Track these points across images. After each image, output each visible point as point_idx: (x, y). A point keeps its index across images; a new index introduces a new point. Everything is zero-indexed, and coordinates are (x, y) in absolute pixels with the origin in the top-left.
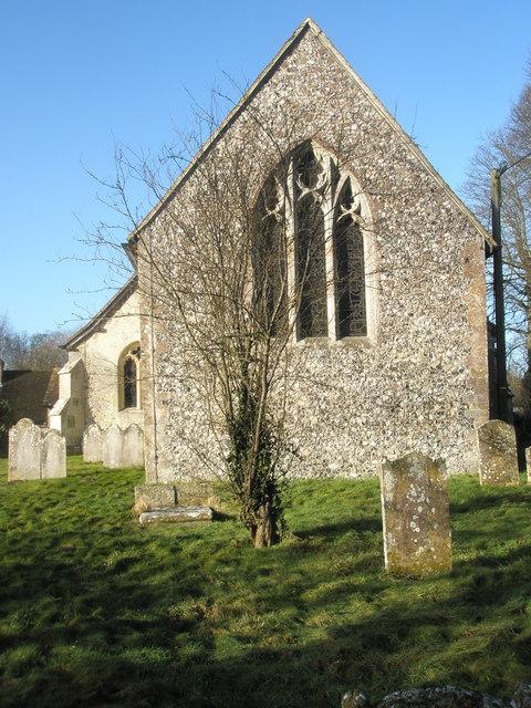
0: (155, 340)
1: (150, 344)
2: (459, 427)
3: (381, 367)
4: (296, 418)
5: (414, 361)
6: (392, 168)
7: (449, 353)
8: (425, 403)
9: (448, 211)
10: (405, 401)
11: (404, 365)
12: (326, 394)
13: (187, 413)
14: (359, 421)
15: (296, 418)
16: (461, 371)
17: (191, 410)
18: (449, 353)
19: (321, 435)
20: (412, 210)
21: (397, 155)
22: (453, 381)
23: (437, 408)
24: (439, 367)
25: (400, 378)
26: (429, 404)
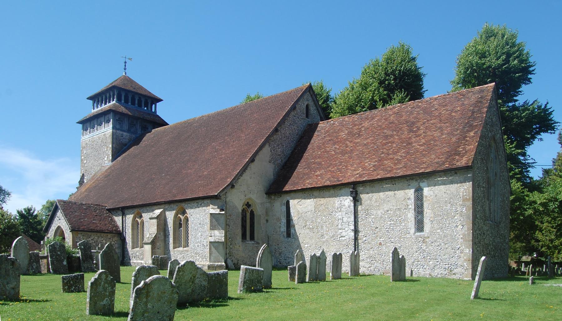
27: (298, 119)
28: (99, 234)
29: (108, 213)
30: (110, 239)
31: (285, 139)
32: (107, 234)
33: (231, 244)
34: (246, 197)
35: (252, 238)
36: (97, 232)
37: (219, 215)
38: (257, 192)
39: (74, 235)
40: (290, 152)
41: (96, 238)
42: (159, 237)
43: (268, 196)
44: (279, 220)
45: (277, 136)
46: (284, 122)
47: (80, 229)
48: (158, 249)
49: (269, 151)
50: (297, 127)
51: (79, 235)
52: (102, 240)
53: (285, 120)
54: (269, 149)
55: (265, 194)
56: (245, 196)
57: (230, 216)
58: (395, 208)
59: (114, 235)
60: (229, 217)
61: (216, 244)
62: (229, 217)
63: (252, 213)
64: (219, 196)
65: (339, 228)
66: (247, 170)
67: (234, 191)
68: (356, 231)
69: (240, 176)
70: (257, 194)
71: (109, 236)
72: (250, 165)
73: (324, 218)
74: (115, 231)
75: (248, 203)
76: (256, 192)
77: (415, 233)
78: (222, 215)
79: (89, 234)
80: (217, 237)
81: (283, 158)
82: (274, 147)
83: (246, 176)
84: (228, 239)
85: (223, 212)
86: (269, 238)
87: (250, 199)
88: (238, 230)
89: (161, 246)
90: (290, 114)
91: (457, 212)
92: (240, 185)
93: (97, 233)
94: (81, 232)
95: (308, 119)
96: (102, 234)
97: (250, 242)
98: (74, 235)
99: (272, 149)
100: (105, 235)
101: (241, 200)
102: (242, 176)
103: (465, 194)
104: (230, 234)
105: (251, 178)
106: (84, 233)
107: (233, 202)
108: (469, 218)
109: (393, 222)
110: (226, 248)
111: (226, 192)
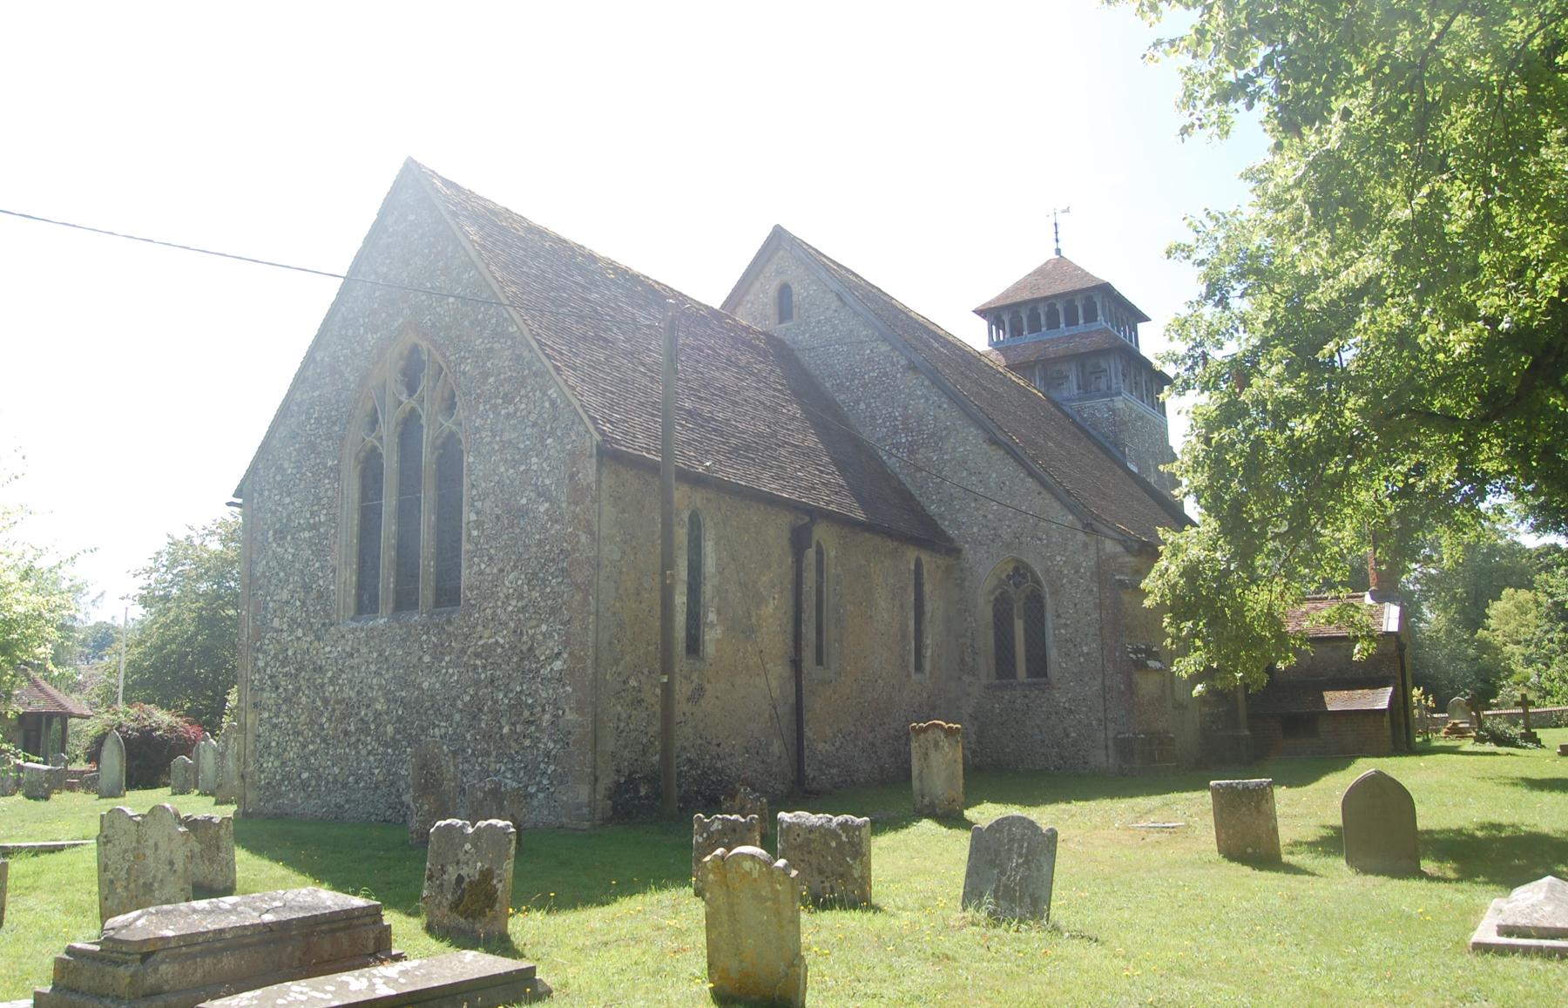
0: (251, 624)
2: (551, 745)
3: (463, 651)
4: (373, 727)
5: (501, 641)
6: (490, 350)
7: (544, 628)
8: (513, 707)
9: (553, 403)
10: (490, 703)
11: (489, 649)
12: (404, 694)
15: (373, 727)
16: (559, 654)
18: (544, 628)
19: (397, 752)
20: (511, 409)
21: (499, 330)
22: (545, 671)
23: (526, 713)
24: (531, 649)
25: (484, 667)
26: (517, 706)
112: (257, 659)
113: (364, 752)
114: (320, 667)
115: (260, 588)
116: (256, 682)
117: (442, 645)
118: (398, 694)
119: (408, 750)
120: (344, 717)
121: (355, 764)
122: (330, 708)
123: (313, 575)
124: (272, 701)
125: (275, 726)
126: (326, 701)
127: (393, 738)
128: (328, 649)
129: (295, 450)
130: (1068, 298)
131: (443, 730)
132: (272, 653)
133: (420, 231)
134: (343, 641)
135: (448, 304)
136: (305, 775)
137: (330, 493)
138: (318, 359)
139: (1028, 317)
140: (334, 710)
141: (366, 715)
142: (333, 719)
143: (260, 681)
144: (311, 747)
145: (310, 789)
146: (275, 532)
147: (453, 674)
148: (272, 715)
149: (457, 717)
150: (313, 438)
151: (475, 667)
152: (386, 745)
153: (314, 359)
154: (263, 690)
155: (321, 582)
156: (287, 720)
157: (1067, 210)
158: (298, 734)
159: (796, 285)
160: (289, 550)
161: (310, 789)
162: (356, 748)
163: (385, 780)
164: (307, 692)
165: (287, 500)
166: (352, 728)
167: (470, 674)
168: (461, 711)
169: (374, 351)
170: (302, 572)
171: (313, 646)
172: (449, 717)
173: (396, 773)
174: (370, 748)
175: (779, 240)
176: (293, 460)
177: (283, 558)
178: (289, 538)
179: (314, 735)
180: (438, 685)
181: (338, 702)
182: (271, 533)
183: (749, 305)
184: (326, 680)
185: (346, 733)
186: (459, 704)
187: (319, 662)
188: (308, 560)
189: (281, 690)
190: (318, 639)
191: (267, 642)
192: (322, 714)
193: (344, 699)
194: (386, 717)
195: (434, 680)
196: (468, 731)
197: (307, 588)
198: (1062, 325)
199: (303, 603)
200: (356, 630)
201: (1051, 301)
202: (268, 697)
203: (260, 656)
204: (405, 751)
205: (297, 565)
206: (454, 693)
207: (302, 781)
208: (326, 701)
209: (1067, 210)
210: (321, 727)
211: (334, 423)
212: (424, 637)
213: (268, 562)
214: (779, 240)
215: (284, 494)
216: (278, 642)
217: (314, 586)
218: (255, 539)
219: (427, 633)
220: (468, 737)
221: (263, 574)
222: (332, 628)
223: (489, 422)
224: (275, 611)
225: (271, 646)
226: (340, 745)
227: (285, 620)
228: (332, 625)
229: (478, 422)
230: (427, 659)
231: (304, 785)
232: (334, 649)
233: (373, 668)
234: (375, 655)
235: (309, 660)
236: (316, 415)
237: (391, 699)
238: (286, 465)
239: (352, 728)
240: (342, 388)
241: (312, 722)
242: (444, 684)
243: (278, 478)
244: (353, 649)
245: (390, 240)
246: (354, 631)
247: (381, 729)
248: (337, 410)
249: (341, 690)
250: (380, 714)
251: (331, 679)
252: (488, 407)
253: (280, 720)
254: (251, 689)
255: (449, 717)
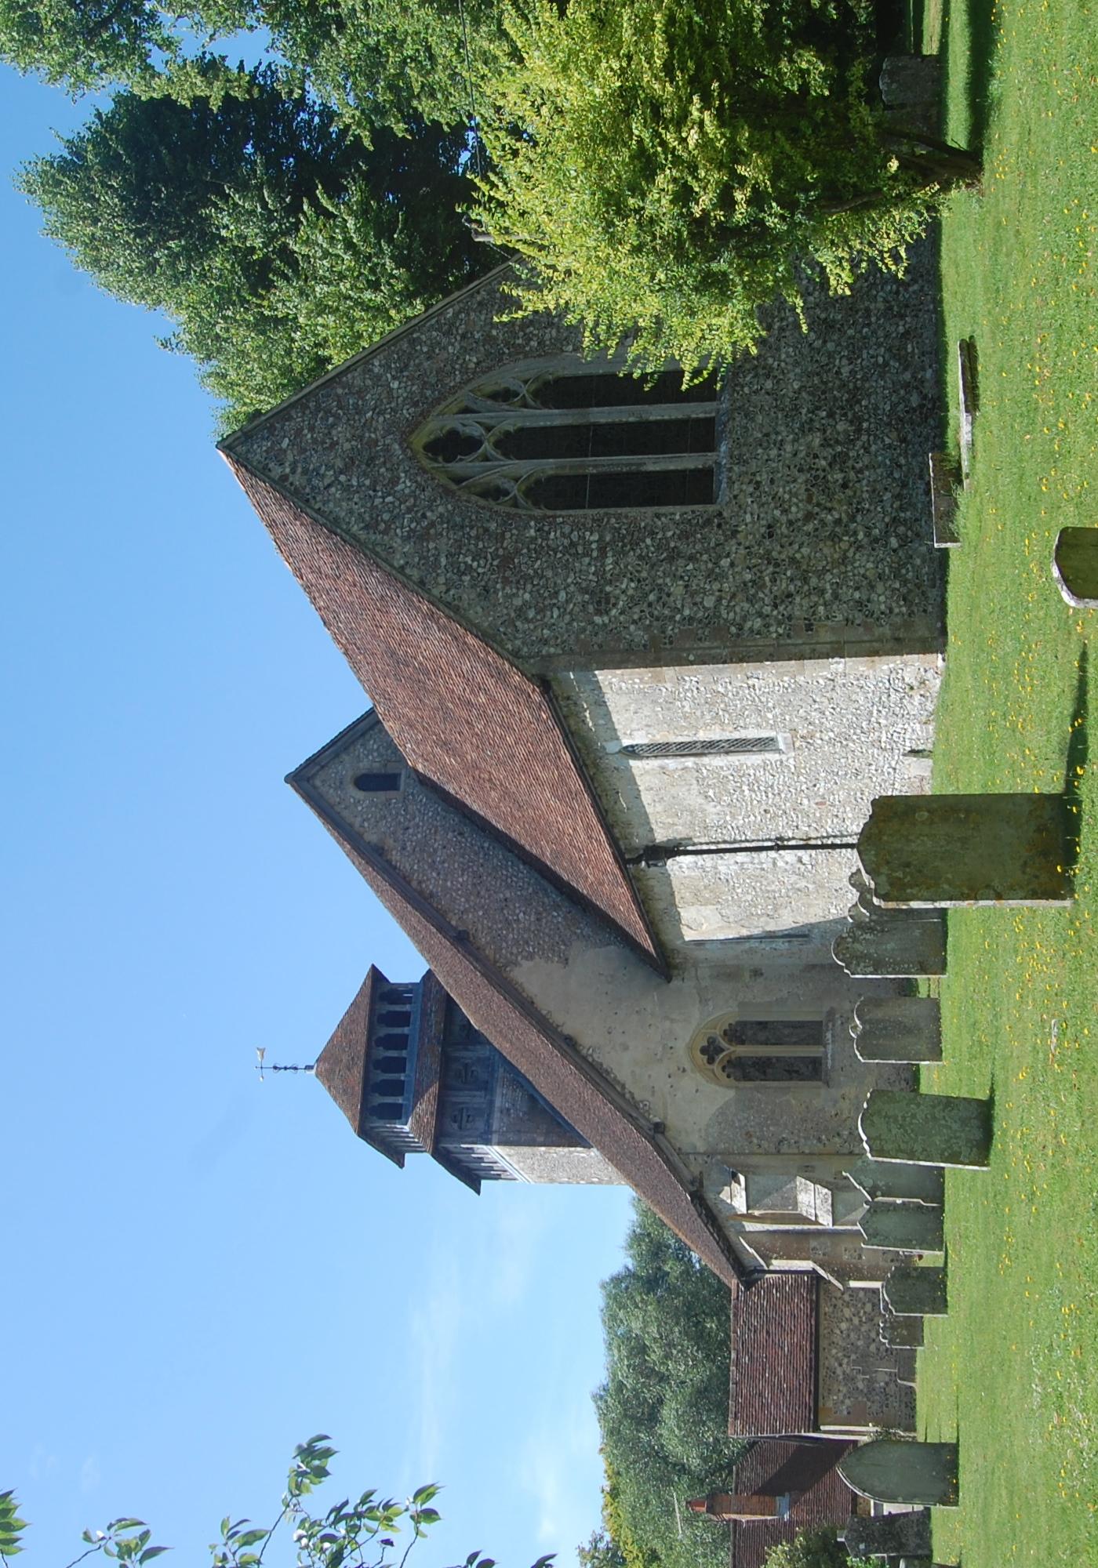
1: (713, 652)
6: (464, 336)
12: (804, 411)
13: (828, 596)
14: (845, 371)
15: (839, 449)
17: (822, 592)
25: (782, 320)
27: (411, 831)
28: (823, 1343)
29: (759, 1292)
30: (835, 1306)
31: (482, 893)
32: (822, 1317)
33: (838, 1134)
34: (687, 1066)
35: (812, 1032)
36: (816, 1351)
37: (750, 1189)
38: (667, 1018)
39: (829, 1420)
40: (521, 867)
41: (834, 1351)
42: (824, 1254)
43: (676, 972)
44: (751, 950)
45: (480, 927)
46: (431, 895)
47: (812, 1405)
48: (860, 1257)
49: (530, 964)
50: (436, 832)
51: (830, 1404)
52: (838, 1332)
53: (421, 893)
54: (526, 964)
55: (669, 979)
56: (684, 1070)
57: (749, 1135)
58: (695, 786)
59: (822, 1293)
60: (755, 1141)
61: (840, 1208)
62: (755, 1141)
63: (737, 1033)
64: (692, 1183)
65: (771, 866)
66: (601, 1064)
67: (673, 1120)
68: (780, 845)
69: (623, 1096)
70: (672, 1021)
71: (826, 1308)
72: (584, 1052)
73: (739, 891)
74: (809, 1292)
75: (704, 1051)
76: (667, 1024)
77: (779, 751)
78: (750, 1182)
79: (822, 1372)
80: (818, 1201)
81: (546, 900)
82: (516, 942)
83: (622, 1065)
84: (820, 1146)
85: (742, 1178)
86: (814, 966)
87: (690, 1049)
88: (793, 1102)
89: (850, 1246)
90: (395, 868)
91: (702, 689)
92: (653, 1092)
93: (821, 1349)
94: (820, 1398)
95: (400, 774)
96: (823, 1331)
97: (830, 1047)
98: (829, 1420)
99: (524, 953)
100: (824, 1323)
101: (697, 1091)
102: (623, 1086)
103: (637, 681)
104: (805, 1138)
105: (626, 1048)
106: (821, 1390)
107: (708, 1125)
108: (720, 670)
109: (745, 788)
110: (851, 1153)
111: (679, 1151)
112: (751, 630)
113: (866, 460)
114: (769, 526)
115: (663, 632)
116: (781, 631)
117: (756, 367)
118: (804, 418)
119: (863, 403)
120: (827, 491)
121: (879, 471)
122: (816, 509)
123: (658, 548)
124: (805, 602)
125: (836, 596)
126: (809, 517)
127: (851, 422)
128: (748, 518)
129: (504, 589)
130: (374, 1041)
131: (845, 362)
132: (746, 605)
133: (306, 431)
134: (741, 496)
135: (399, 388)
136: (894, 542)
137: (567, 529)
138: (402, 562)
139: (385, 1071)
140: (818, 505)
141: (825, 458)
142: (829, 505)
143: (779, 624)
144: (861, 536)
145: (909, 533)
146: (599, 612)
147: (787, 353)
148: (821, 601)
149: (830, 346)
150: (495, 563)
151: (782, 329)
152: (859, 431)
153: (402, 567)
154: (790, 618)
155: (670, 534)
156: (828, 576)
157: (262, 1051)
158: (844, 560)
159: (361, 765)
160: (624, 586)
161: (909, 533)
162: (861, 471)
163: (897, 429)
164: (796, 546)
165: (562, 595)
166: (839, 476)
167: (788, 333)
168: (825, 342)
169: (419, 479)
170: (653, 566)
171: (742, 541)
172: (830, 355)
173: (888, 416)
174: (862, 451)
175: (303, 779)
176: (514, 591)
177: (632, 597)
178: (608, 589)
179: (846, 533)
180: (798, 370)
181: (809, 500)
182: (598, 620)
183: (366, 824)
184: (784, 519)
185: (845, 486)
186: (818, 344)
187: (763, 530)
188: (640, 557)
189: (792, 588)
190: (735, 533)
191: (732, 615)
192: (823, 522)
193: (807, 490)
194: (828, 432)
195: (791, 376)
196: (845, 333)
197: (674, 556)
198: (406, 1030)
199: (692, 558)
200: (730, 478)
201: (372, 1064)
202: (800, 607)
203: (749, 624)
204: (866, 407)
205: (644, 574)
206: (805, 351)
207: (901, 546)
208: (809, 517)
209: (262, 1051)
210: (838, 522)
211: (486, 530)
212: (746, 390)
213: (634, 622)
214: (303, 779)
215: (555, 601)
216: (734, 596)
217: (672, 545)
218: (600, 646)
219: (743, 387)
220: (851, 332)
221: (647, 629)
222: (725, 514)
223: (536, 332)
224: (695, 604)
225: (737, 609)
226: (858, 493)
227: (708, 587)
228: (720, 514)
229: (534, 344)
230: (769, 384)
231: (904, 541)
232: (749, 509)
233: (774, 453)
234: (760, 451)
235: (759, 545)
236: (469, 560)
237: (807, 428)
238: (518, 602)
239: (839, 476)
240: (448, 523)
241: (834, 538)
242: (797, 364)
243: (531, 614)
244: (750, 482)
245: (299, 470)
246: (731, 482)
247: (841, 438)
248: (472, 528)
249: (796, 495)
250: (825, 439)
251: (785, 511)
252: (521, 334)
253: (828, 586)
254: (789, 636)
255: (830, 355)
